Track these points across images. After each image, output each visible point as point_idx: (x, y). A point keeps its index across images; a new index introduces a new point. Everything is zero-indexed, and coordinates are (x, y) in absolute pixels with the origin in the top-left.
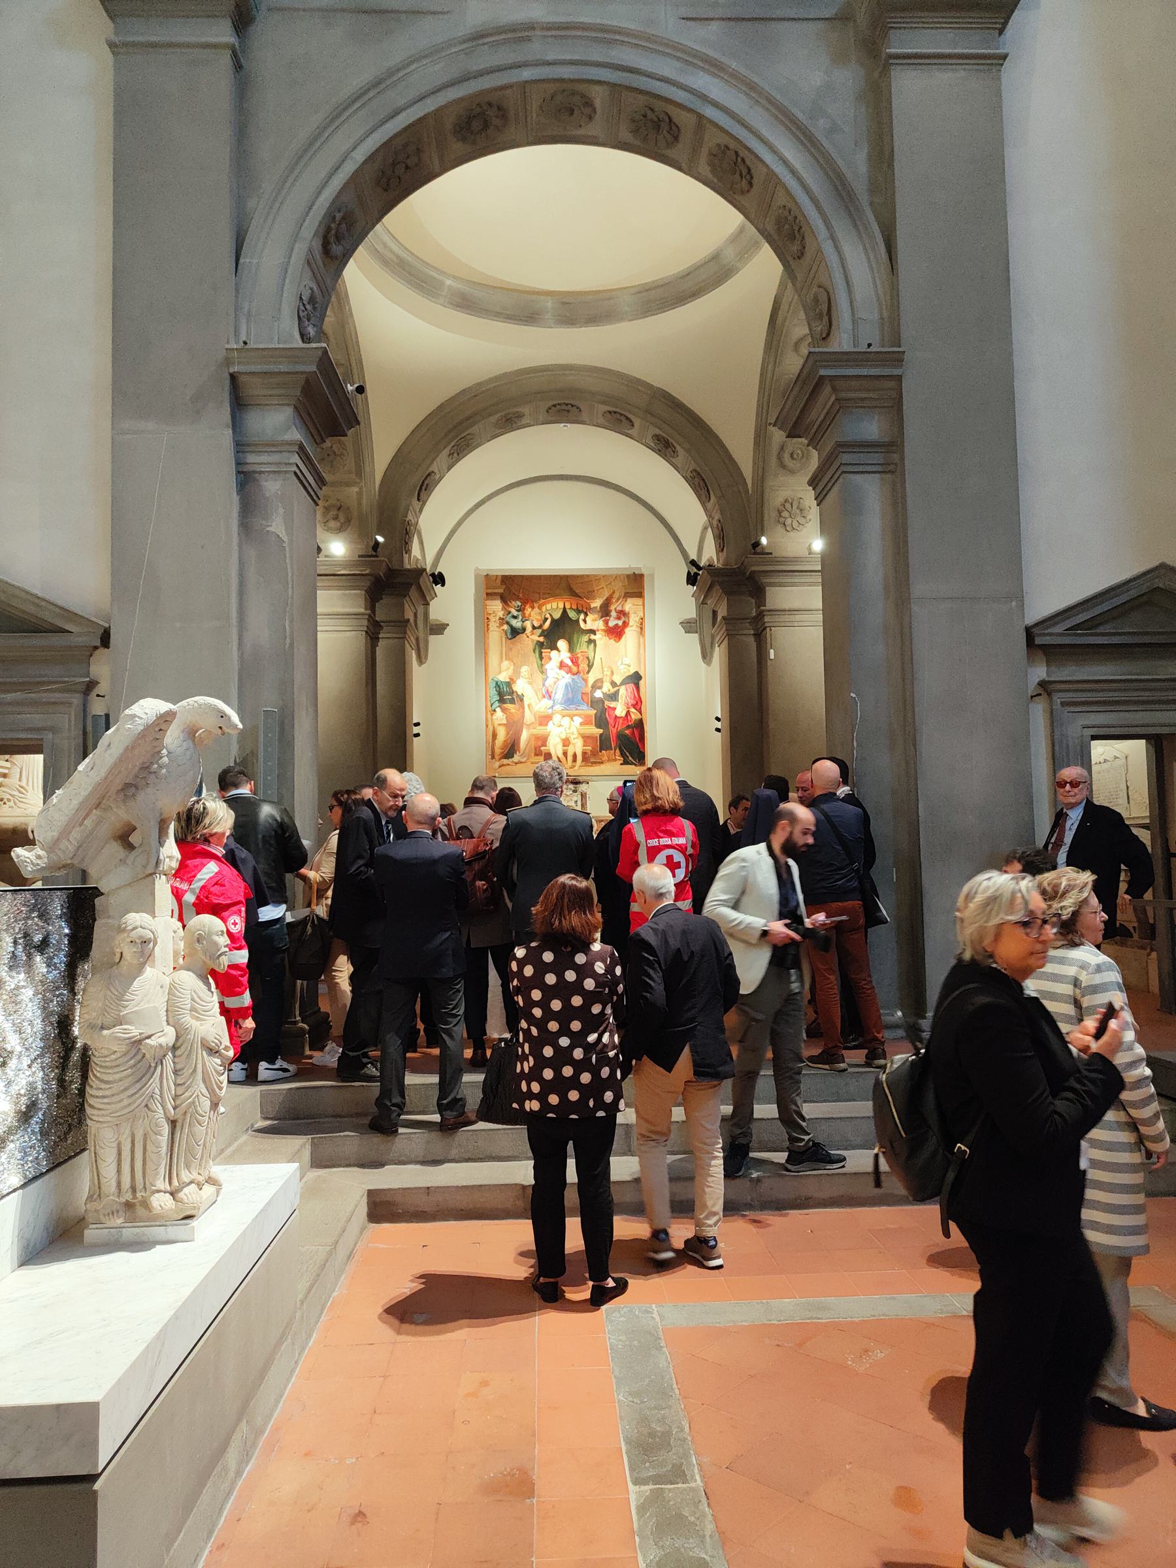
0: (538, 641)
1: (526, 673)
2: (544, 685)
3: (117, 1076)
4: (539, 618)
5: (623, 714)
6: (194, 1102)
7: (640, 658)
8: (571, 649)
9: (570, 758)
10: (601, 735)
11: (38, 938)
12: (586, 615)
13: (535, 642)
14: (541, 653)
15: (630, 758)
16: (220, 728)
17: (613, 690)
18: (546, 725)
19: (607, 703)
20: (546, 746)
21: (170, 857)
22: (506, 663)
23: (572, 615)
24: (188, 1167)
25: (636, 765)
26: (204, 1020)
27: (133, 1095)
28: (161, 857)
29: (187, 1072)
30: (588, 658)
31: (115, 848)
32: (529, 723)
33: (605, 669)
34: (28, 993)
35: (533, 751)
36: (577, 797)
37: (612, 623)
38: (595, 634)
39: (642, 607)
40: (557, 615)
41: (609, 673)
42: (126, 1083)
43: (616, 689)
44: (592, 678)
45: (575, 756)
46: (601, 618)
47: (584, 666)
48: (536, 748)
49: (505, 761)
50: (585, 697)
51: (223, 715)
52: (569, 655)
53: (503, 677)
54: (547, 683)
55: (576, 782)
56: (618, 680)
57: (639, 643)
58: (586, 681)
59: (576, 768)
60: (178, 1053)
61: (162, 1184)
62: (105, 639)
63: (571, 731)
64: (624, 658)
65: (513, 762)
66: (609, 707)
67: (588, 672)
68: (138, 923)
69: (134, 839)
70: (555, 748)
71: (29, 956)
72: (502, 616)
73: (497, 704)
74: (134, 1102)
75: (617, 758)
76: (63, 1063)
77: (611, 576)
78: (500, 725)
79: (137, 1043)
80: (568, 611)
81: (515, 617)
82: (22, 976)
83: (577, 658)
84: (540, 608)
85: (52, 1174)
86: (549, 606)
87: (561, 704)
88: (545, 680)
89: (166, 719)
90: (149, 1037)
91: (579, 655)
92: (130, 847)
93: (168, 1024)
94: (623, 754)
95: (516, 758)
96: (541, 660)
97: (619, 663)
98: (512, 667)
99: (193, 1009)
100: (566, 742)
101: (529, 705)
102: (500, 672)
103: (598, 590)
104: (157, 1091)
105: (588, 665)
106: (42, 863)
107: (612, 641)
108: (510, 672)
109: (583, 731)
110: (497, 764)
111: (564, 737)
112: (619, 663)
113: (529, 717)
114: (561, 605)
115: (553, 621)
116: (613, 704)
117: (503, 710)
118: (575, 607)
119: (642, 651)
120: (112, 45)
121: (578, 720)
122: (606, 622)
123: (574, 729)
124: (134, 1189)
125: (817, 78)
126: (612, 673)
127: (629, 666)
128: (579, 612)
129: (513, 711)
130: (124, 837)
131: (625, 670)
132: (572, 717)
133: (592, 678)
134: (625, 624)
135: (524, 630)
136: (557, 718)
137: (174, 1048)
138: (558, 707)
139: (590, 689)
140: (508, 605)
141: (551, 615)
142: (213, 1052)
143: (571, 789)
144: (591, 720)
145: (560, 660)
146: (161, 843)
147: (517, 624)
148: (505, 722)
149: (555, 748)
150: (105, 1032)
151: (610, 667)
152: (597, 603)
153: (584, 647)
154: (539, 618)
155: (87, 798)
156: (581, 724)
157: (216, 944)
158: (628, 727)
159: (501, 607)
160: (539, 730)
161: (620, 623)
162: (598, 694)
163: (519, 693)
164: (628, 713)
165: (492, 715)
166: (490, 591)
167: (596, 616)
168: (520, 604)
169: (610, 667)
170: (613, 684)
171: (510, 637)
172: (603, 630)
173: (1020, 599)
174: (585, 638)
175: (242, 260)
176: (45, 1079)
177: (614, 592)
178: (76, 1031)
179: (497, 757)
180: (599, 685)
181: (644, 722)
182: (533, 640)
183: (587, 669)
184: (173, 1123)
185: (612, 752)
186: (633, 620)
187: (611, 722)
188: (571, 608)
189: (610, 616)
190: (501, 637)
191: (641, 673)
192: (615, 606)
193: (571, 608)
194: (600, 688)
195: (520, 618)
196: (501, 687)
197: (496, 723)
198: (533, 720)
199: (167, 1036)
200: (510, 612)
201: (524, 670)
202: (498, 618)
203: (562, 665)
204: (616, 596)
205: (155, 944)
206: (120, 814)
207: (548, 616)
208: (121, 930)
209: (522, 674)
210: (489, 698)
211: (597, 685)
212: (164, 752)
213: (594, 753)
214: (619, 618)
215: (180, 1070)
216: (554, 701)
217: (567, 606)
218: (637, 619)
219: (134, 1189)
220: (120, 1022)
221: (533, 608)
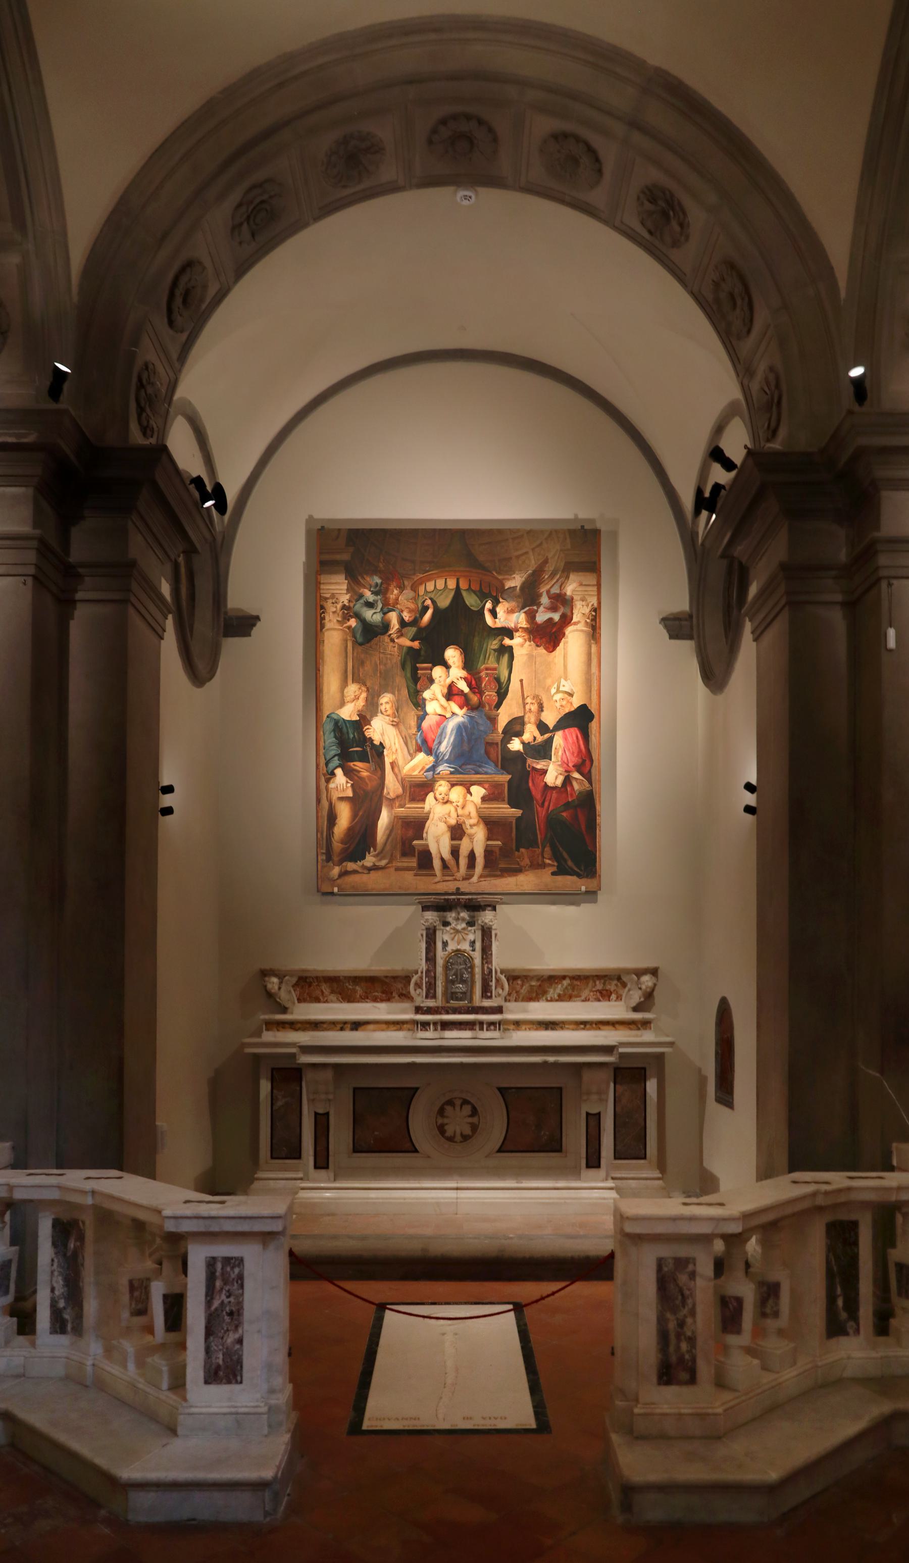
0: (410, 649)
1: (388, 707)
2: (419, 727)
4: (412, 606)
5: (559, 782)
7: (590, 681)
8: (468, 664)
9: (463, 862)
10: (518, 819)
12: (496, 602)
13: (405, 650)
14: (415, 670)
15: (570, 863)
17: (540, 739)
18: (423, 800)
19: (530, 761)
20: (421, 838)
22: (352, 689)
23: (471, 600)
25: (579, 876)
30: (498, 680)
32: (392, 795)
33: (529, 700)
35: (399, 846)
36: (473, 934)
37: (542, 617)
38: (512, 638)
39: (595, 589)
40: (444, 602)
41: (534, 708)
43: (547, 736)
44: (504, 717)
45: (472, 856)
46: (523, 608)
47: (490, 695)
48: (403, 843)
49: (351, 866)
50: (492, 751)
52: (463, 673)
53: (348, 713)
54: (425, 724)
55: (474, 907)
56: (551, 721)
57: (589, 654)
58: (493, 720)
59: (475, 879)
63: (466, 811)
64: (563, 682)
65: (363, 867)
66: (534, 768)
67: (498, 705)
70: (438, 842)
72: (346, 603)
73: (336, 761)
75: (548, 861)
77: (542, 532)
78: (341, 799)
80: (464, 594)
81: (370, 605)
83: (479, 680)
84: (414, 588)
86: (430, 586)
87: (447, 762)
88: (421, 718)
91: (483, 674)
94: (556, 856)
95: (369, 860)
96: (416, 683)
97: (553, 691)
98: (364, 695)
100: (457, 832)
101: (393, 765)
102: (342, 704)
103: (518, 557)
105: (498, 693)
107: (542, 651)
108: (361, 703)
109: (487, 812)
110: (336, 871)
111: (453, 822)
112: (553, 691)
113: (392, 786)
114: (452, 584)
115: (437, 610)
116: (540, 765)
117: (348, 773)
118: (476, 587)
119: (594, 669)
121: (478, 792)
122: (531, 616)
123: (471, 809)
126: (541, 708)
127: (571, 695)
128: (483, 596)
129: (365, 774)
131: (564, 703)
132: (467, 786)
133: (504, 717)
134: (566, 620)
135: (386, 626)
136: (442, 787)
138: (444, 769)
139: (501, 736)
140: (358, 583)
141: (433, 602)
143: (463, 919)
144: (502, 793)
145: (448, 681)
147: (372, 616)
148: (350, 793)
149: (438, 842)
151: (536, 697)
152: (515, 581)
153: (491, 663)
154: (412, 606)
156: (484, 799)
158: (567, 806)
159: (345, 587)
160: (410, 809)
161: (556, 617)
162: (516, 745)
163: (377, 743)
164: (568, 780)
165: (328, 781)
166: (326, 557)
167: (513, 604)
168: (379, 581)
169: (536, 697)
170: (542, 727)
171: (360, 639)
172: (525, 630)
174: (494, 644)
177: (546, 562)
179: (336, 859)
180: (517, 728)
181: (596, 797)
182: (401, 647)
183: (495, 698)
185: (538, 851)
186: (580, 613)
187: (537, 794)
188: (469, 589)
189: (539, 605)
190: (346, 641)
191: (593, 708)
192: (548, 587)
193: (469, 589)
194: (519, 734)
195: (380, 605)
196: (345, 729)
197: (335, 795)
198: (400, 791)
200: (361, 596)
201: (386, 700)
202: (339, 606)
203: (451, 693)
204: (550, 568)
207: (428, 602)
209: (383, 708)
210: (322, 751)
211: (515, 728)
213: (505, 852)
214: (553, 609)
216: (437, 757)
217: (463, 585)
218: (587, 610)
221: (402, 588)
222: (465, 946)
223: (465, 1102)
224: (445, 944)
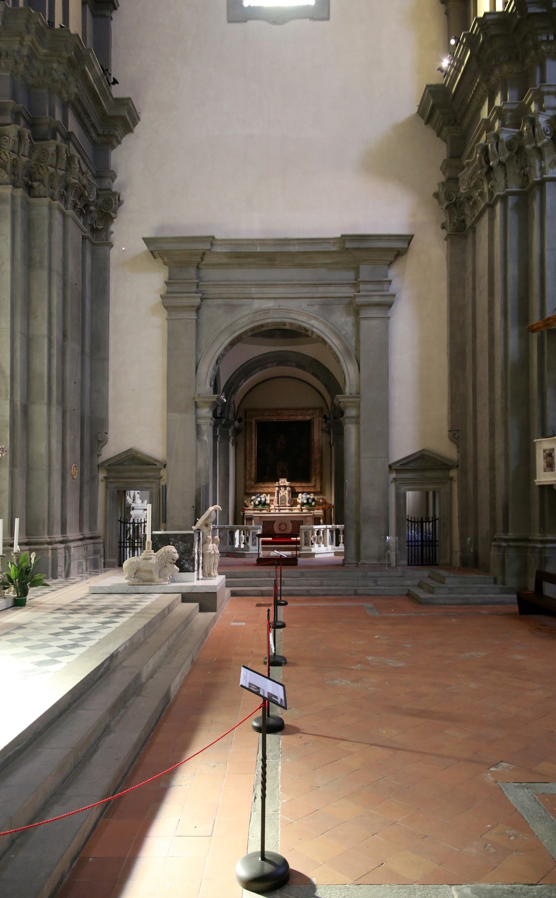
51: (219, 508)
61: (213, 572)
62: (165, 466)
79: (210, 553)
120: (167, 319)
125: (343, 320)
137: (214, 554)
142: (218, 555)
173: (388, 460)
175: (197, 371)
199: (213, 552)
220: (208, 550)
222: (284, 494)
223: (284, 523)
224: (280, 494)
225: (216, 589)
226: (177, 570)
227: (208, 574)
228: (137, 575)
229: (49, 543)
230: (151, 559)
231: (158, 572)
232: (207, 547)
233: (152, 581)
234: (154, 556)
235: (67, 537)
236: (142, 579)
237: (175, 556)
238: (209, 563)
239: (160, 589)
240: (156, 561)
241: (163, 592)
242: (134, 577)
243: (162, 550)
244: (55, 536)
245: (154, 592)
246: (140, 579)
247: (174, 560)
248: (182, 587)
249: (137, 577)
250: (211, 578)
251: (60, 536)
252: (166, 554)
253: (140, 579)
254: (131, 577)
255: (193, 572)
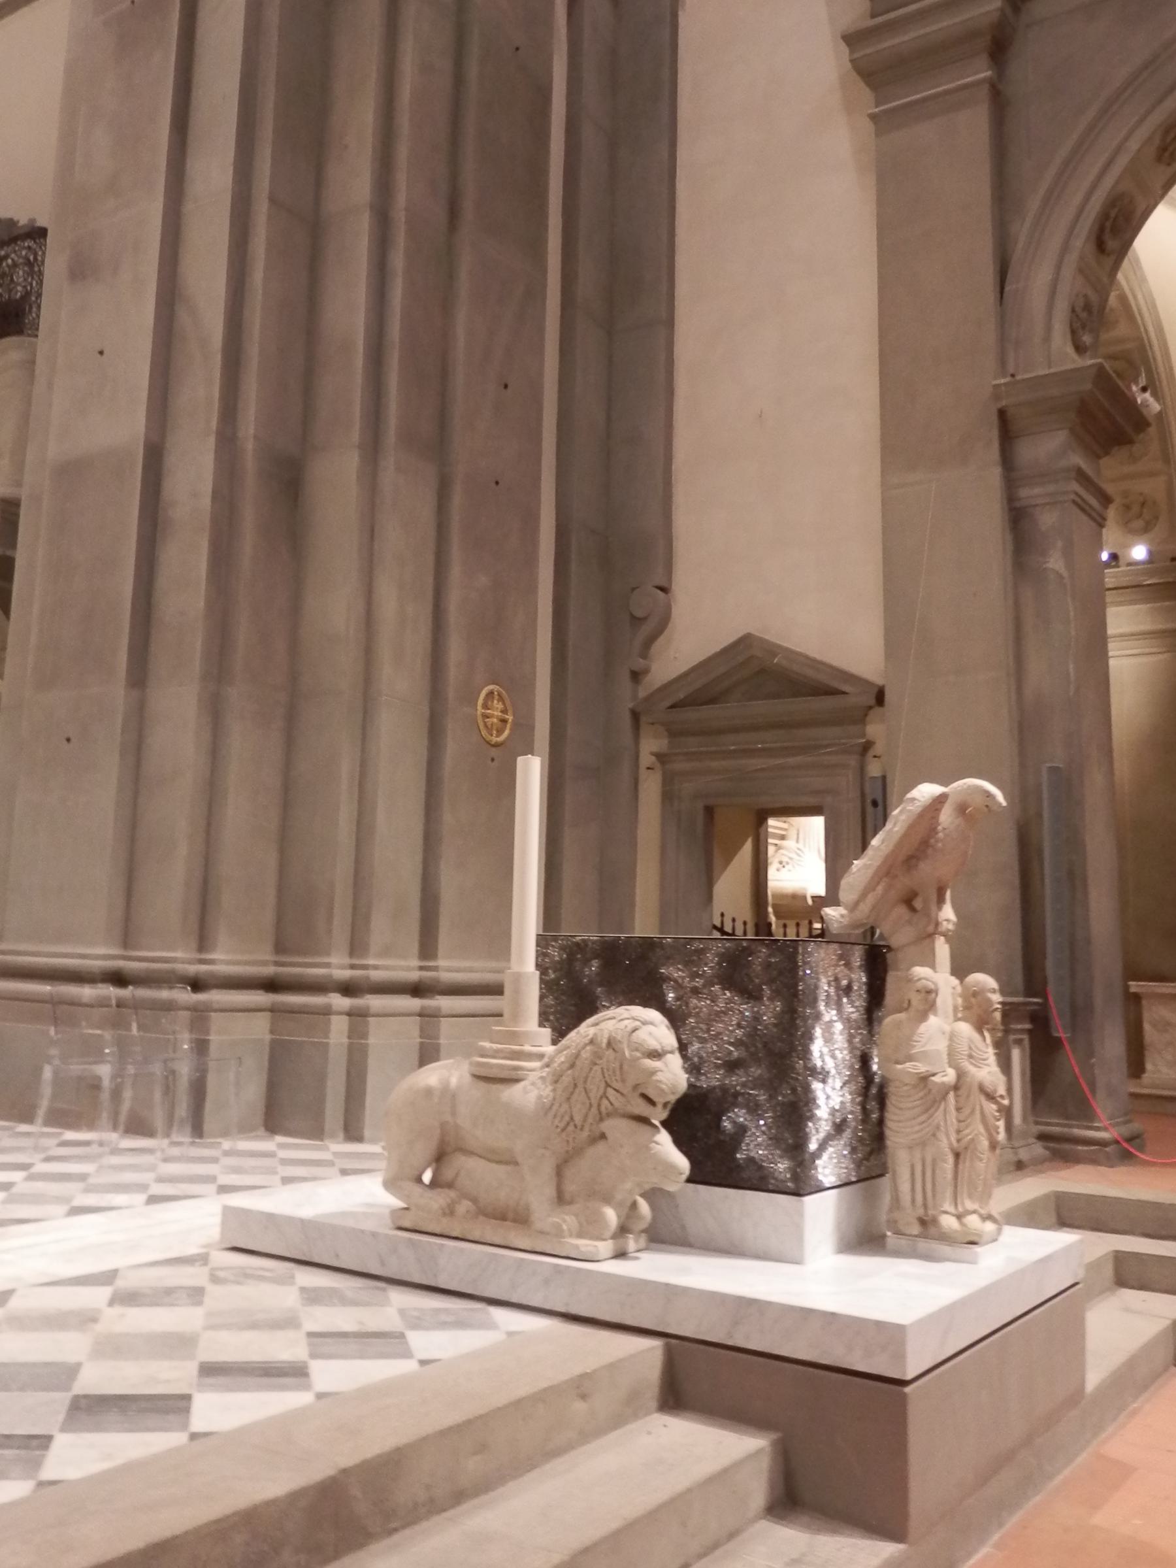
3: (910, 1105)
6: (973, 1140)
11: (844, 982)
16: (987, 806)
21: (948, 920)
24: (970, 1196)
26: (980, 1067)
27: (923, 1122)
28: (940, 920)
29: (967, 1111)
31: (902, 910)
34: (839, 1026)
42: (917, 1111)
51: (989, 795)
60: (959, 1093)
61: (948, 1206)
68: (922, 976)
69: (918, 904)
71: (838, 995)
74: (922, 1130)
76: (865, 1092)
79: (924, 1079)
82: (834, 1012)
85: (859, 1185)
89: (941, 800)
90: (934, 1075)
92: (913, 910)
93: (950, 1066)
99: (970, 1056)
104: (942, 1124)
106: (845, 921)
124: (925, 1206)
130: (908, 901)
137: (956, 1088)
142: (990, 1097)
146: (940, 908)
150: (899, 1067)
155: (879, 867)
157: (989, 1001)
176: (853, 1100)
178: (875, 1067)
184: (957, 1155)
199: (949, 1076)
205: (937, 994)
206: (904, 882)
208: (909, 980)
212: (940, 828)
215: (961, 1109)
219: (925, 1206)
220: (910, 1058)
225: (900, 1356)
226: (671, 1168)
227: (923, 1222)
228: (448, 1174)
229: (348, 989)
230: (517, 1081)
231: (548, 1168)
232: (909, 1040)
233: (519, 1218)
234: (536, 1064)
235: (436, 969)
236: (474, 1200)
237: (653, 1072)
238: (923, 1144)
239: (547, 1282)
240: (540, 1097)
241: (562, 1309)
242: (434, 1184)
243: (586, 1029)
244: (371, 962)
245: (514, 1300)
246: (465, 1195)
247: (652, 1102)
248: (671, 1292)
249: (450, 1185)
250: (945, 1249)
251: (416, 963)
252: (597, 1055)
253: (465, 1195)
254: (419, 1180)
255: (797, 1194)
